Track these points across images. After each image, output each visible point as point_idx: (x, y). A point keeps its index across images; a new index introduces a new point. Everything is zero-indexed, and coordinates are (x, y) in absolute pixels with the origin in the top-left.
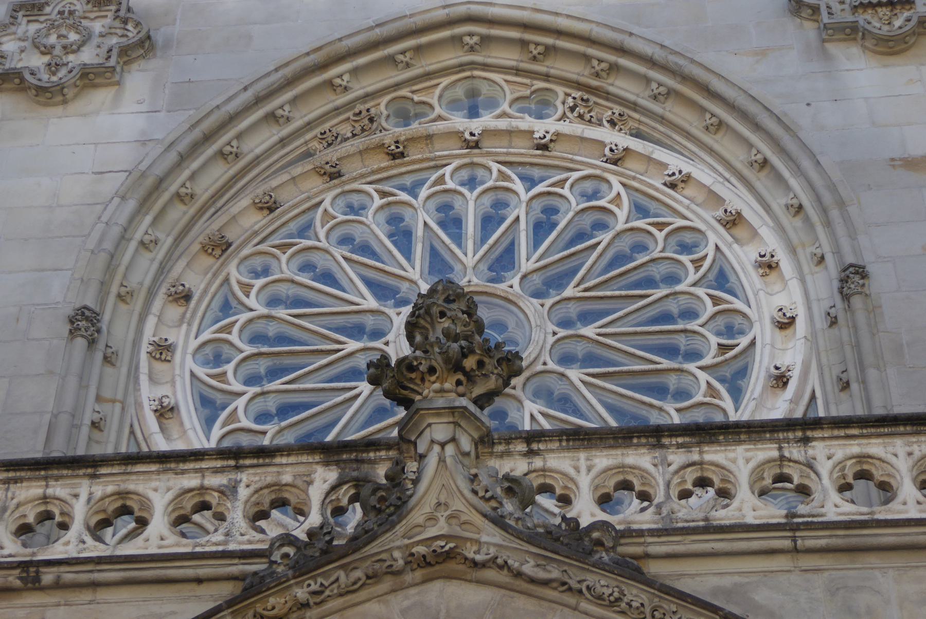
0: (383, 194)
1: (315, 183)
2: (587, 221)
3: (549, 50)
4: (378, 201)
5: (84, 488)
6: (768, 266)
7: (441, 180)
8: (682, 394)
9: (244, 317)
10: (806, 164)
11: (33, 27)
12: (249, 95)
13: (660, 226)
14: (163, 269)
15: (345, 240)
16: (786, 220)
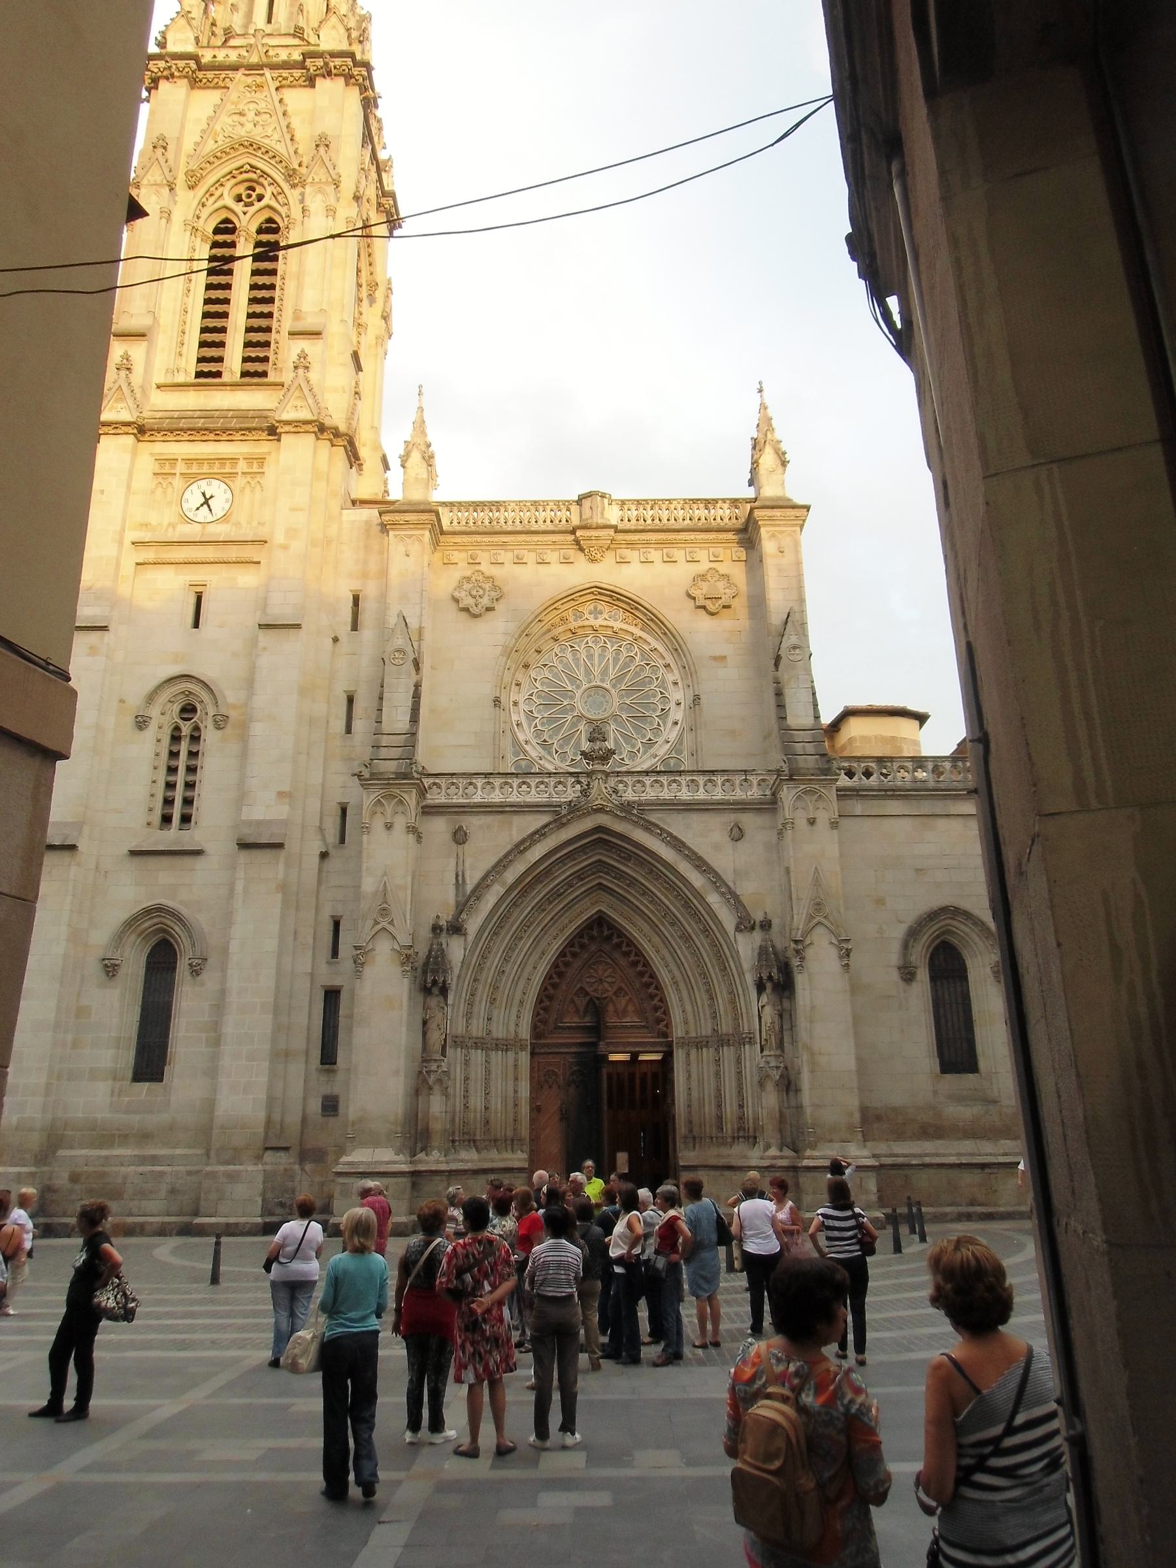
0: (572, 647)
1: (551, 642)
2: (628, 659)
3: (618, 599)
4: (570, 649)
5: (515, 780)
6: (676, 683)
7: (587, 643)
8: (651, 723)
9: (536, 690)
10: (688, 656)
11: (467, 586)
12: (533, 616)
13: (648, 664)
14: (514, 675)
15: (561, 662)
16: (681, 669)
